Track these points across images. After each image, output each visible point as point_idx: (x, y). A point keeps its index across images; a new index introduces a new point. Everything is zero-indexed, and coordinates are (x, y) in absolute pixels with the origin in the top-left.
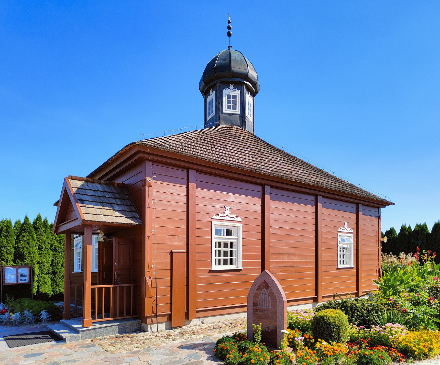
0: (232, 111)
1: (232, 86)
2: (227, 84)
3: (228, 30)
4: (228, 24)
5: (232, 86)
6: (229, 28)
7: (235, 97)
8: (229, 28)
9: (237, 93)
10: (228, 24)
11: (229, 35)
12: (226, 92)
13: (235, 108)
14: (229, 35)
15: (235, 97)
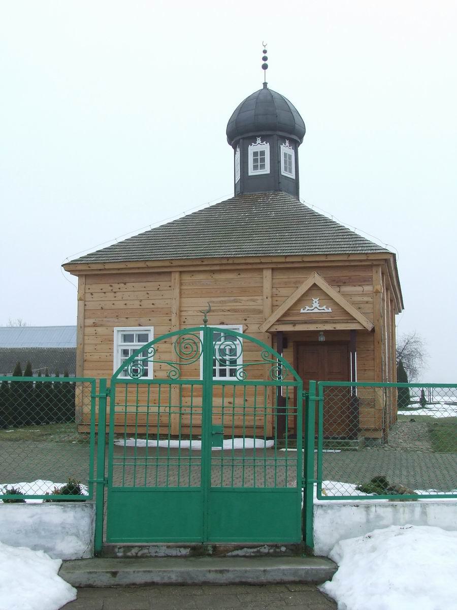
0: (259, 172)
1: (259, 141)
2: (253, 140)
3: (263, 62)
4: (263, 55)
5: (259, 141)
6: (265, 59)
7: (263, 153)
8: (265, 59)
9: (266, 147)
10: (263, 55)
11: (265, 67)
12: (252, 149)
13: (263, 167)
14: (265, 67)
15: (263, 153)
